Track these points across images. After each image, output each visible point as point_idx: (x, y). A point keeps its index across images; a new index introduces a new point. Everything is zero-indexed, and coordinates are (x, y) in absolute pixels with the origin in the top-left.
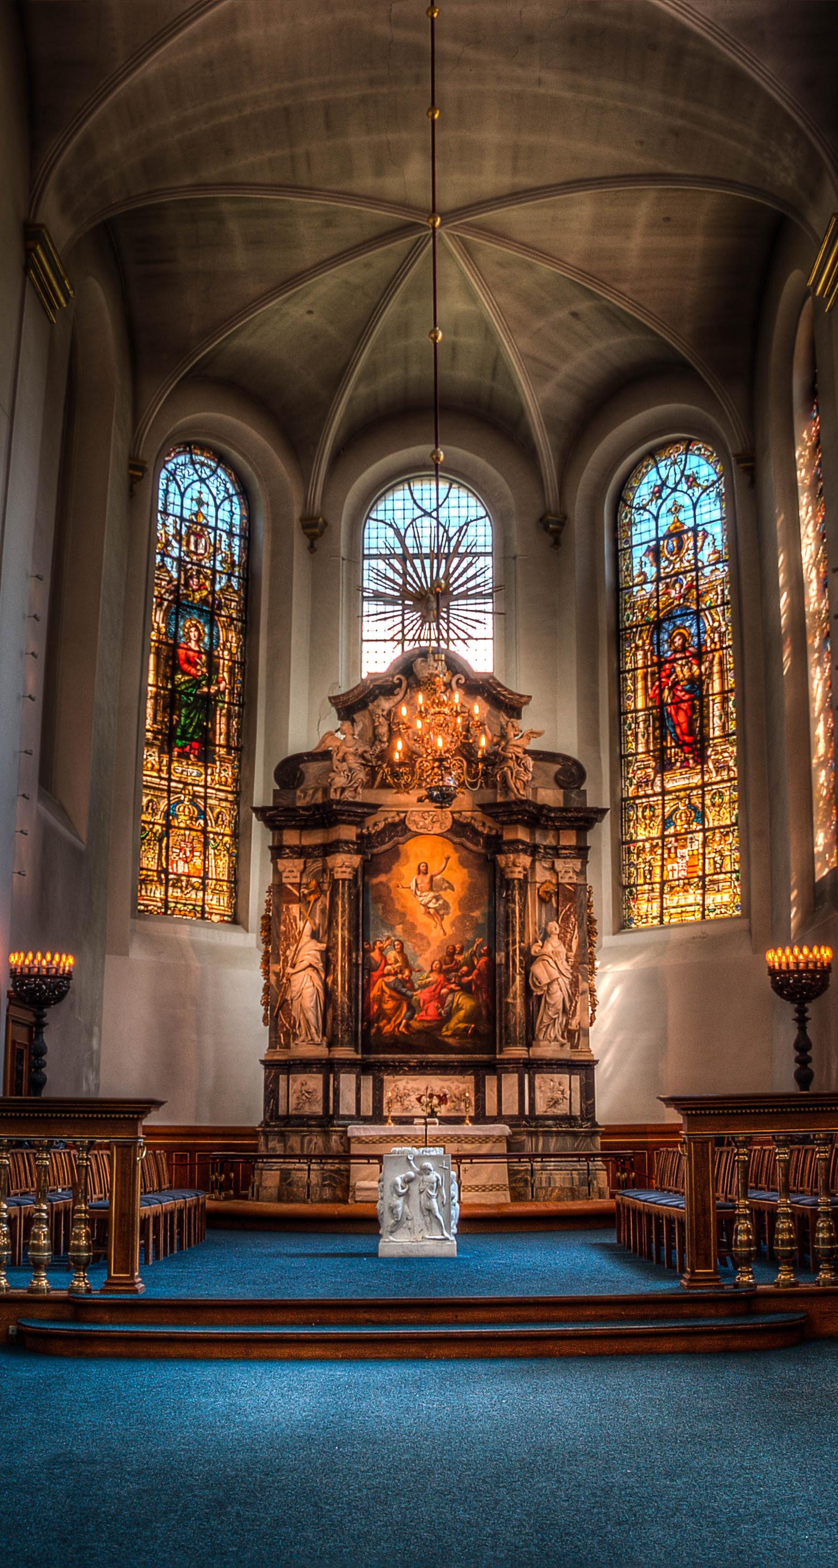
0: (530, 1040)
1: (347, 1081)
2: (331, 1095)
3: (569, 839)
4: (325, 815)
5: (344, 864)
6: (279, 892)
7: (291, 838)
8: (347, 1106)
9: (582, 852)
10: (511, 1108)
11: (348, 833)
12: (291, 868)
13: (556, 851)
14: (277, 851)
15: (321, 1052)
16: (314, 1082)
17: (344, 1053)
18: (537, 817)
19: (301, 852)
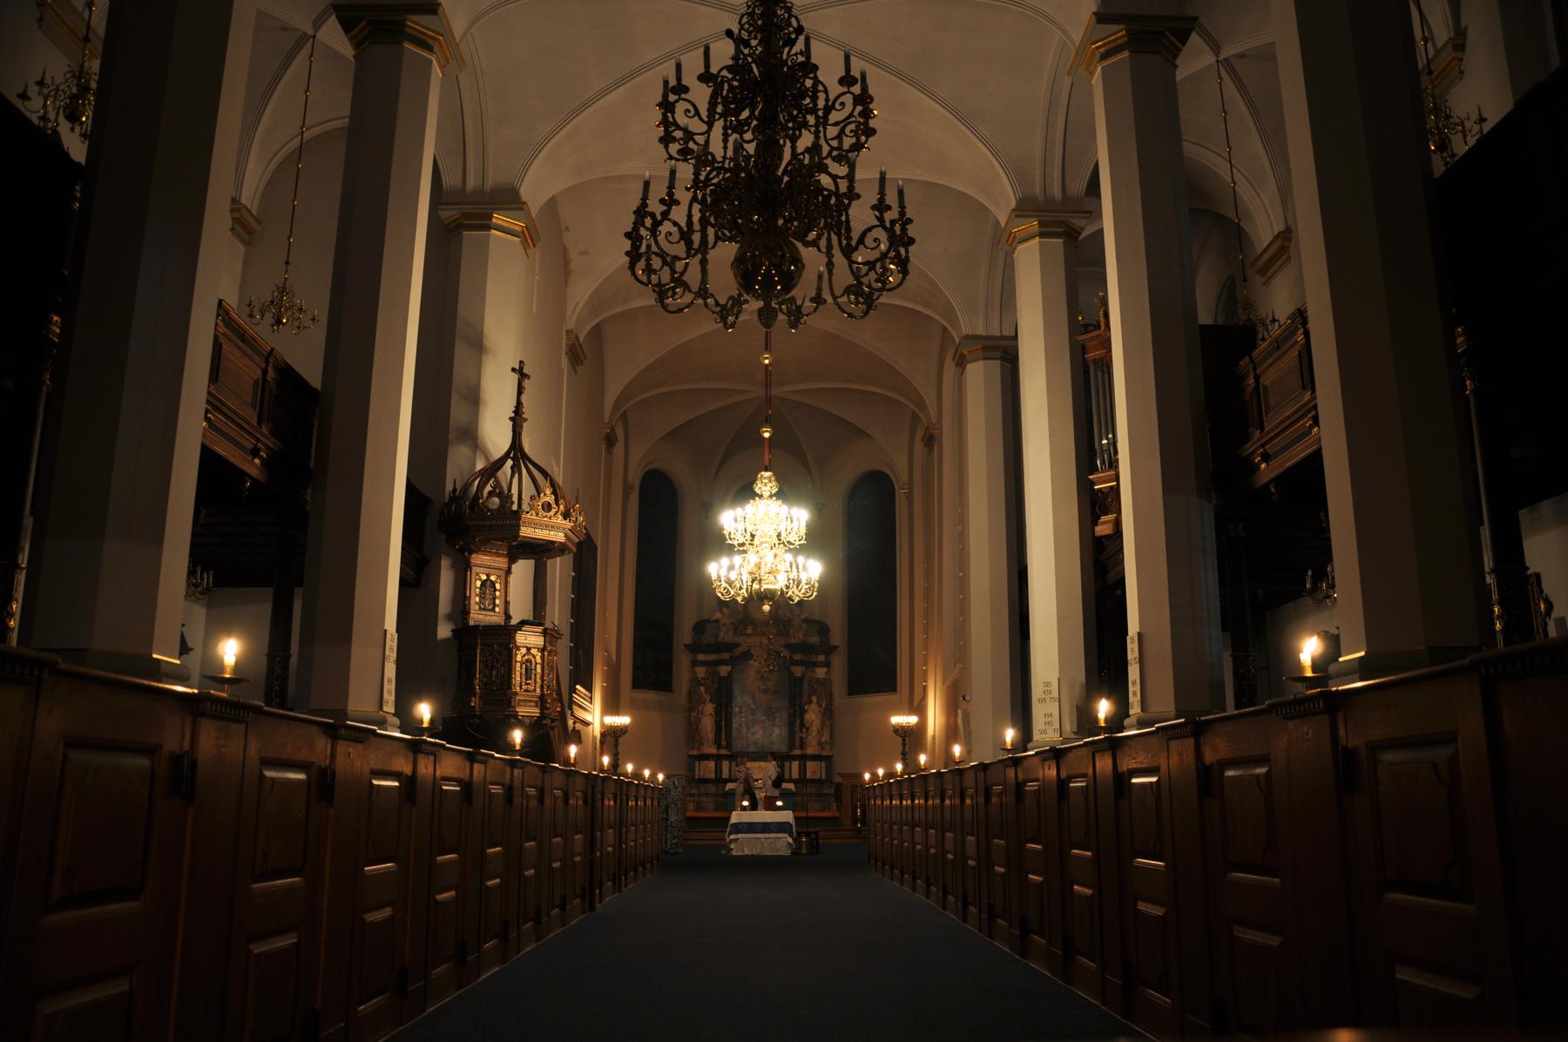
0: (802, 747)
1: (725, 764)
2: (718, 770)
3: (822, 658)
4: (717, 647)
5: (724, 670)
6: (695, 682)
7: (701, 657)
8: (725, 775)
9: (827, 664)
10: (795, 775)
11: (726, 656)
12: (701, 672)
13: (816, 664)
14: (695, 663)
15: (713, 751)
16: (711, 764)
17: (723, 752)
18: (805, 648)
19: (705, 663)
